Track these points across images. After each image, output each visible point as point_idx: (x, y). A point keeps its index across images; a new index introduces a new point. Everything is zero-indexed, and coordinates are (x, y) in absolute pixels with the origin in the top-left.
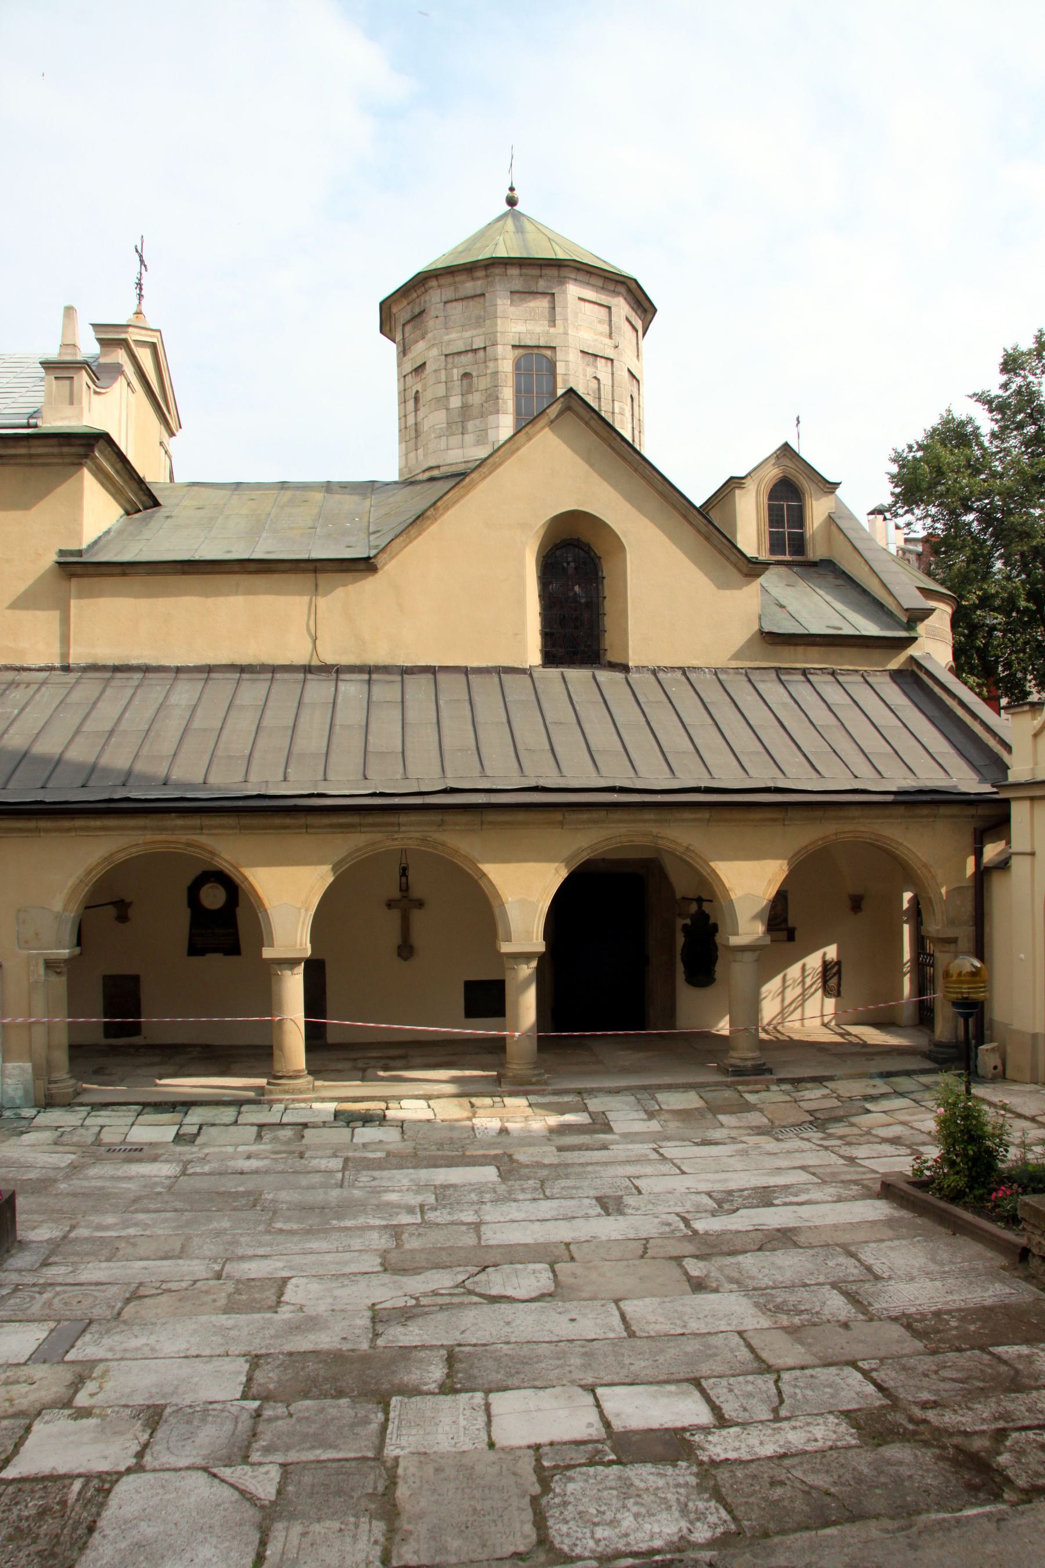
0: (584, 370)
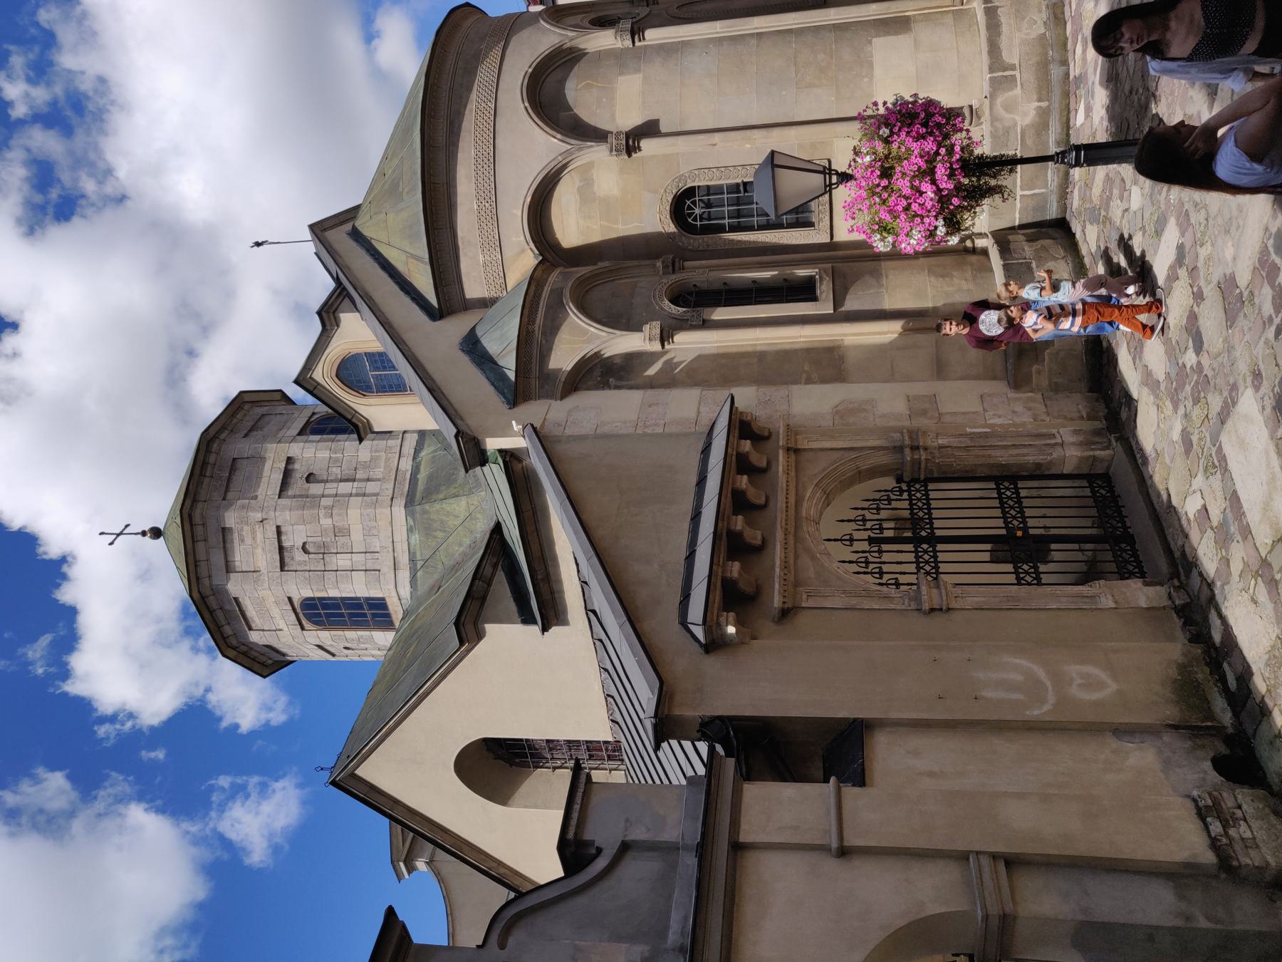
0: (300, 563)
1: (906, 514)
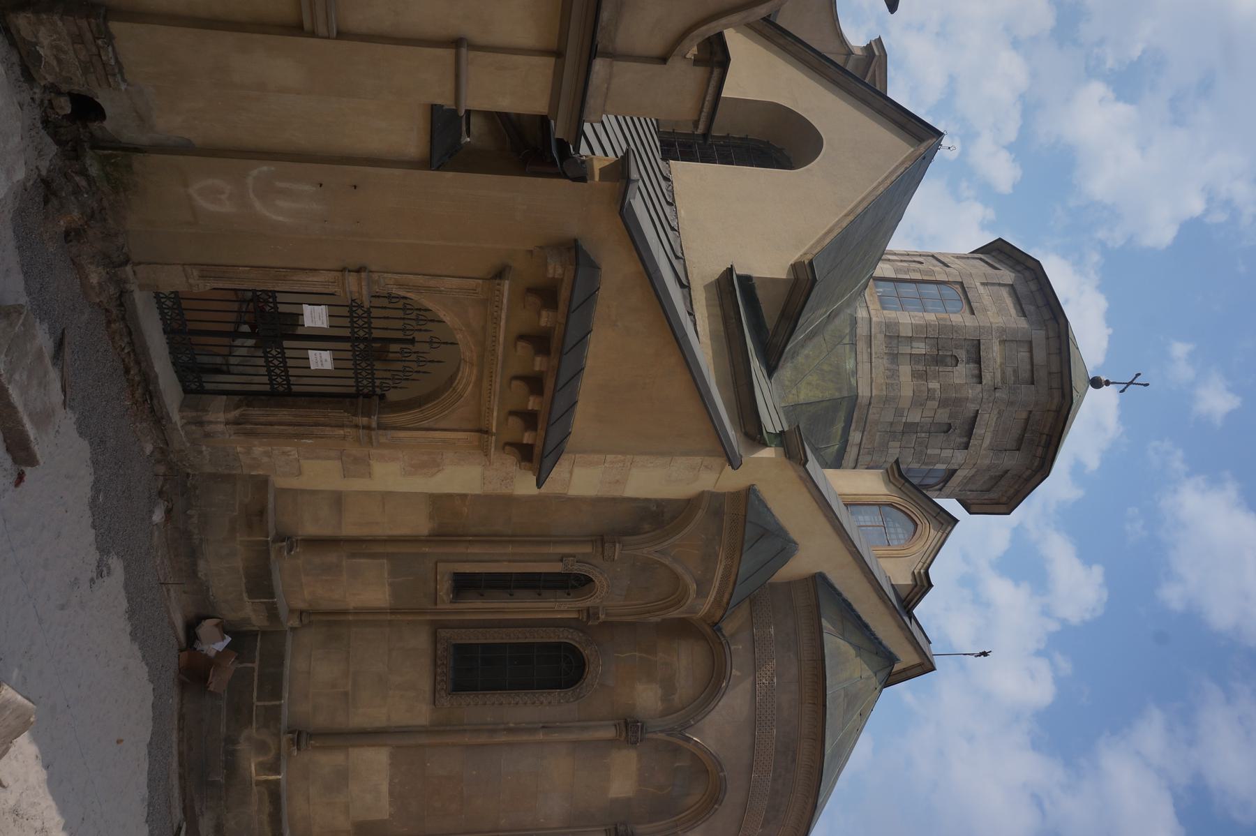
1: (378, 365)
